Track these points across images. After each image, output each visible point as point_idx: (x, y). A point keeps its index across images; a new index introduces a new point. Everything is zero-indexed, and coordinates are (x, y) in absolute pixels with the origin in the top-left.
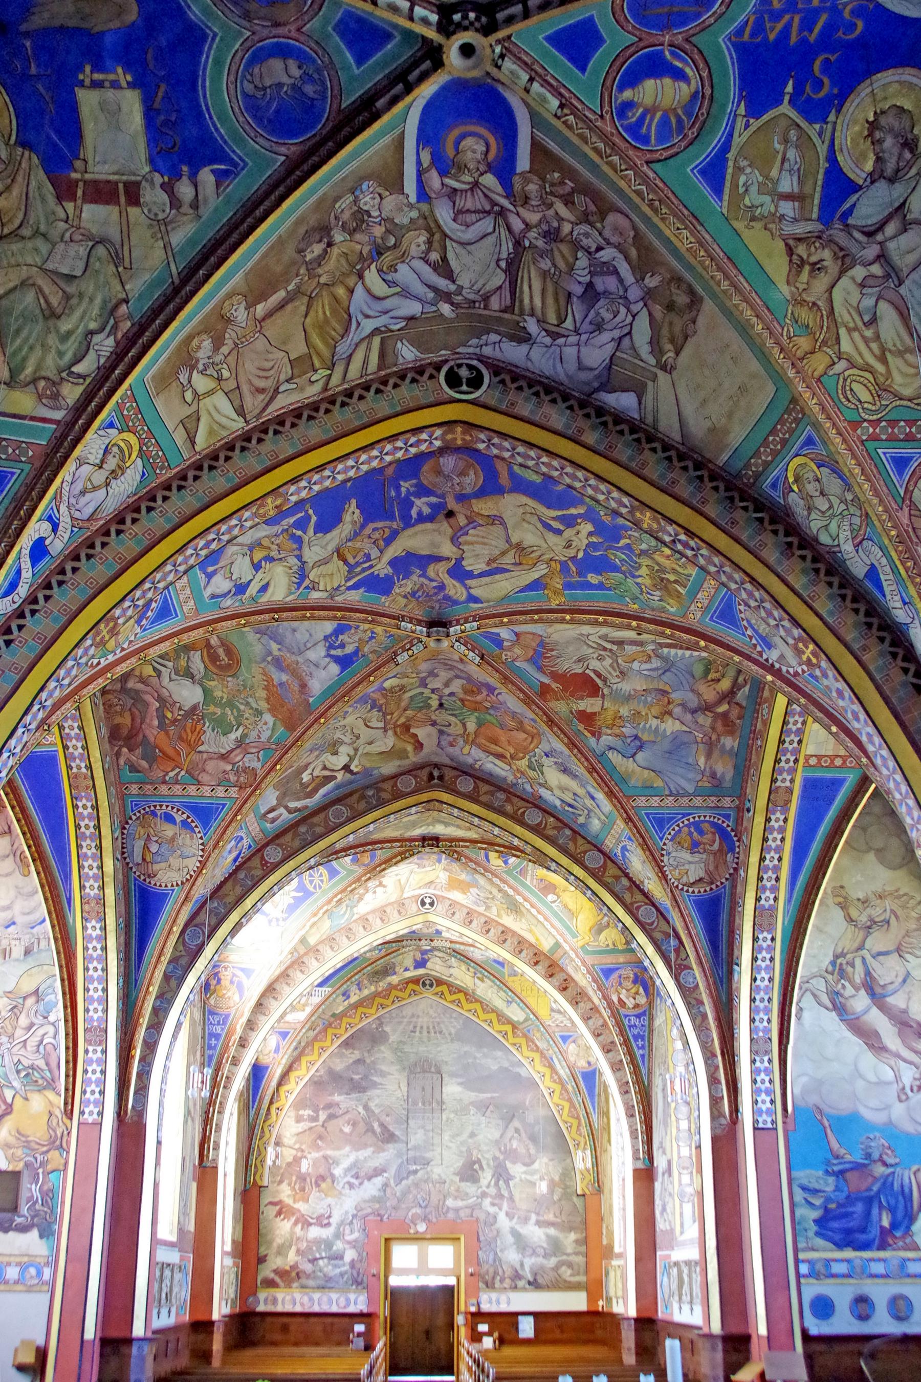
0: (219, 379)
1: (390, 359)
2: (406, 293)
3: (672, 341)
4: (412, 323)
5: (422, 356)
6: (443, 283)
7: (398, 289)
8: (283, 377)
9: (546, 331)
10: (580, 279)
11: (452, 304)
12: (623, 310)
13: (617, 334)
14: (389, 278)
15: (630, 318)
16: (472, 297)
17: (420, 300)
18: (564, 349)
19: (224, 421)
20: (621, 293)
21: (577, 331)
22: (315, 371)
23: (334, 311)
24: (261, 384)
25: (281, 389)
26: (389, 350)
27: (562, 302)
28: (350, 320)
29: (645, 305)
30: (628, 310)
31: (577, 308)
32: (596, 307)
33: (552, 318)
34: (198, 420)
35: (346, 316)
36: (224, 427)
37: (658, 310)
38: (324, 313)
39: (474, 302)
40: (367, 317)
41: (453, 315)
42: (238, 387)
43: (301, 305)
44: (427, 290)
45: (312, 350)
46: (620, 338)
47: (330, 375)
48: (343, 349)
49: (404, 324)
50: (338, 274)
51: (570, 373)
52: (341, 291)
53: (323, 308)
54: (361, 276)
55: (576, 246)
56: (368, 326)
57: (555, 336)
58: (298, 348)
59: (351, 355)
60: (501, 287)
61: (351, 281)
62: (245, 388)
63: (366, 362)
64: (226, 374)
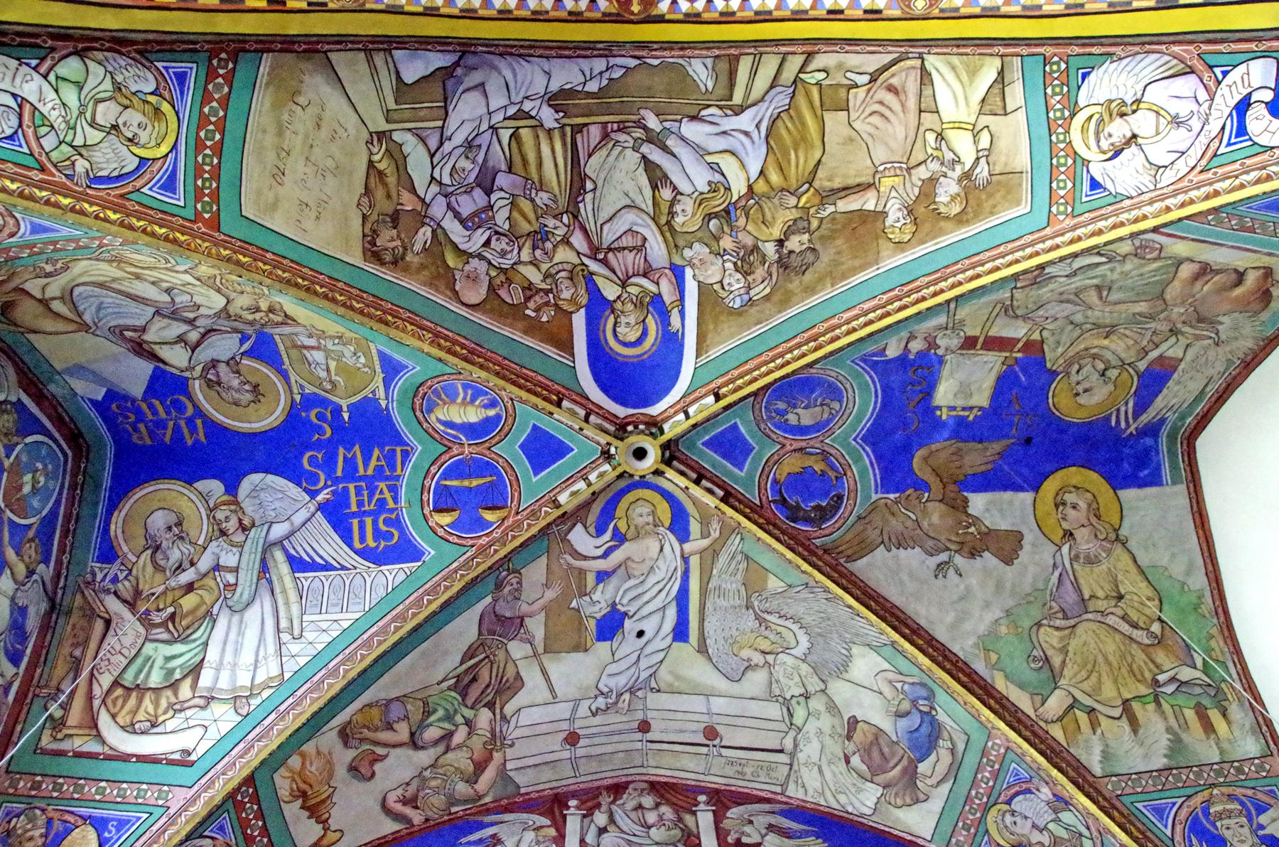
0: (940, 136)
1: (723, 66)
2: (700, 152)
3: (381, 174)
4: (694, 113)
5: (680, 61)
6: (656, 156)
7: (709, 159)
8: (861, 92)
9: (532, 117)
10: (502, 194)
11: (645, 128)
12: (446, 180)
13: (447, 147)
14: (718, 177)
15: (436, 175)
16: (622, 137)
17: (683, 139)
18: (506, 102)
19: (950, 76)
20: (453, 199)
21: (494, 129)
22: (818, 84)
23: (786, 154)
24: (889, 98)
25: (866, 78)
26: (724, 79)
27: (517, 159)
28: (767, 137)
29: (423, 200)
30: (440, 183)
31: (498, 158)
32: (477, 170)
33: (525, 133)
34: (983, 100)
35: (772, 143)
36: (953, 68)
37: (408, 202)
38: (797, 157)
39: (619, 130)
40: (746, 134)
41: (642, 112)
42: (920, 111)
43: (822, 181)
44: (675, 150)
45: (819, 112)
46: (441, 144)
47: (802, 70)
48: (780, 99)
49: (704, 113)
50: (776, 201)
51: (495, 74)
52: (775, 178)
53: (799, 163)
54: (750, 187)
55: (513, 236)
56: (745, 121)
57: (522, 115)
58: (834, 121)
59: (772, 87)
60: (590, 156)
61: (761, 187)
62: (912, 103)
63: (754, 73)
64: (931, 137)
